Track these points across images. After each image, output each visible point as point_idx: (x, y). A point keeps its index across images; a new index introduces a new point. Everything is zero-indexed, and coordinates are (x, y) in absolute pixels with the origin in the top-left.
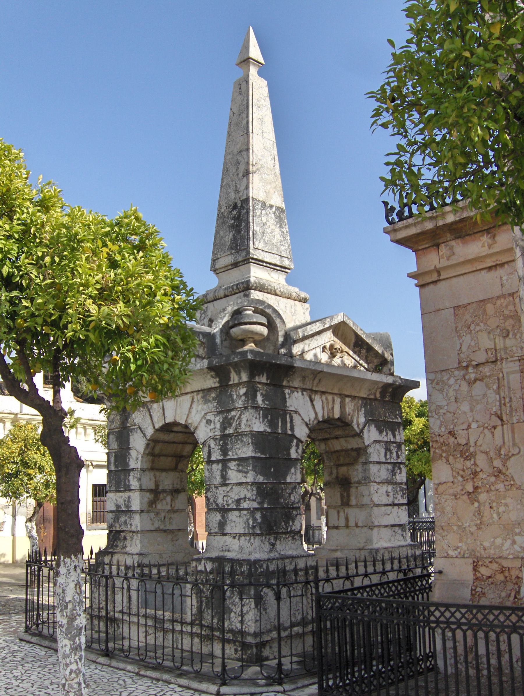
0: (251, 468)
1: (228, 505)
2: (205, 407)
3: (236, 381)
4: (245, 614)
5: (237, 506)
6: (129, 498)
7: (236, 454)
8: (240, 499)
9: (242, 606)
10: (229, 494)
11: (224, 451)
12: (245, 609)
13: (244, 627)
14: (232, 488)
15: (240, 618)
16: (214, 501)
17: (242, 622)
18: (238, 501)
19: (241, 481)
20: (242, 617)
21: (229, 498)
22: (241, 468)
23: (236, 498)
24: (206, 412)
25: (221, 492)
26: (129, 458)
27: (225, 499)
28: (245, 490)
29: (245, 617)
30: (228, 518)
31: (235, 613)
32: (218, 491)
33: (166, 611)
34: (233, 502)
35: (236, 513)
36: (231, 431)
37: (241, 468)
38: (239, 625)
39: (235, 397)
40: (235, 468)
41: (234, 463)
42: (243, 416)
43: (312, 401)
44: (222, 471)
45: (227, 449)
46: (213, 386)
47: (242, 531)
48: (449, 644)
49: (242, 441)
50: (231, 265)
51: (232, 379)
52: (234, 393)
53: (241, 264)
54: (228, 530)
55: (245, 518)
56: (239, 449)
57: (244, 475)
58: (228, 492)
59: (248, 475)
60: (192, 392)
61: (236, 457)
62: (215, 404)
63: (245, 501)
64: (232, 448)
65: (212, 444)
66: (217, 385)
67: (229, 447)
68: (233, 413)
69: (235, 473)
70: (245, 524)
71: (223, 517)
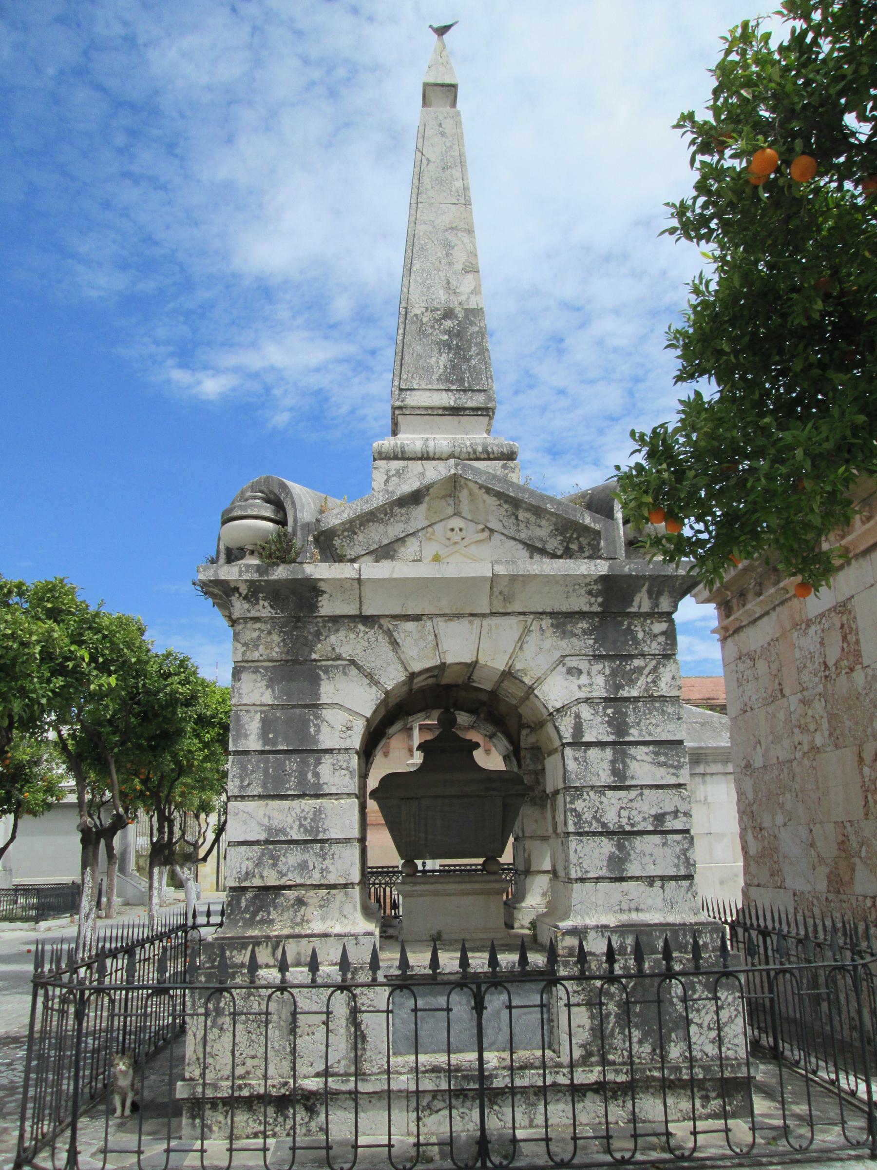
0: (687, 760)
1: (632, 825)
2: (563, 643)
3: (646, 607)
4: (725, 1024)
5: (656, 826)
6: (317, 812)
7: (650, 734)
8: (664, 815)
9: (718, 1009)
10: (634, 804)
11: (619, 725)
12: (724, 1015)
13: (724, 1049)
14: (641, 794)
15: (713, 1034)
16: (594, 817)
17: (719, 1041)
18: (659, 818)
19: (664, 782)
20: (719, 1029)
21: (634, 813)
22: (662, 759)
23: (653, 812)
24: (567, 653)
25: (613, 801)
26: (317, 727)
27: (624, 813)
28: (676, 798)
29: (726, 1029)
30: (633, 848)
31: (700, 1026)
32: (603, 799)
33: (492, 1047)
34: (644, 819)
35: (656, 839)
36: (635, 693)
37: (662, 759)
38: (711, 1050)
39: (640, 635)
40: (649, 759)
41: (643, 749)
42: (662, 669)
43: (395, 644)
44: (613, 762)
45: (627, 724)
46: (586, 609)
47: (672, 872)
48: (789, 987)
49: (663, 712)
50: (445, 408)
51: (636, 603)
52: (638, 628)
53: (467, 412)
54: (633, 869)
55: (678, 849)
56: (657, 726)
57: (674, 771)
58: (631, 801)
59: (682, 771)
60: (524, 614)
61: (648, 738)
62: (591, 642)
63: (676, 817)
64: (638, 724)
65: (586, 712)
66: (596, 608)
67: (631, 719)
68: (637, 662)
69: (647, 767)
70: (678, 858)
71: (620, 847)
